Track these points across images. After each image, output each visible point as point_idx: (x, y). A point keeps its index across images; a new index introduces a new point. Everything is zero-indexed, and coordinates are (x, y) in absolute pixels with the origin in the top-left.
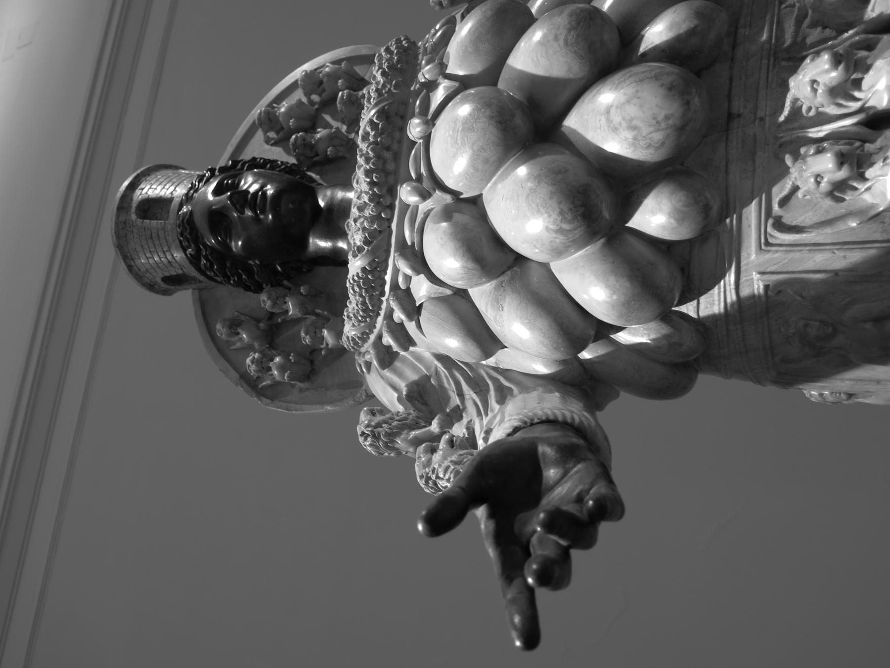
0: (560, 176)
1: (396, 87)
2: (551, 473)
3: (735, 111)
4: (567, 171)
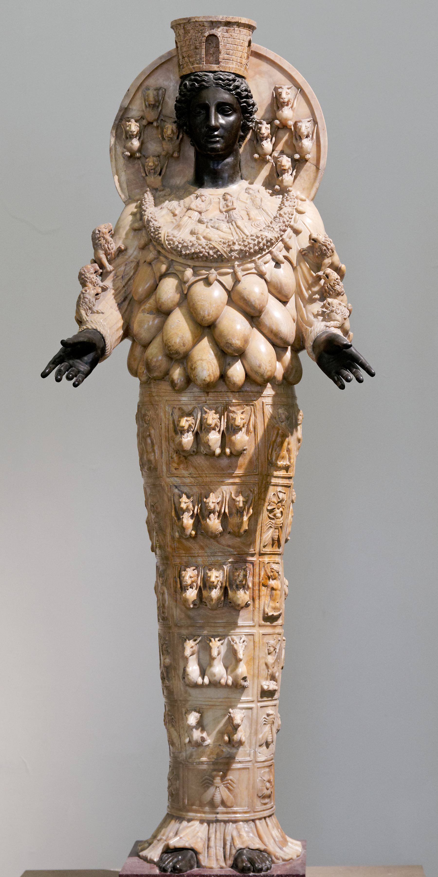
0: (182, 344)
1: (235, 257)
2: (86, 358)
3: (210, 393)
4: (184, 346)
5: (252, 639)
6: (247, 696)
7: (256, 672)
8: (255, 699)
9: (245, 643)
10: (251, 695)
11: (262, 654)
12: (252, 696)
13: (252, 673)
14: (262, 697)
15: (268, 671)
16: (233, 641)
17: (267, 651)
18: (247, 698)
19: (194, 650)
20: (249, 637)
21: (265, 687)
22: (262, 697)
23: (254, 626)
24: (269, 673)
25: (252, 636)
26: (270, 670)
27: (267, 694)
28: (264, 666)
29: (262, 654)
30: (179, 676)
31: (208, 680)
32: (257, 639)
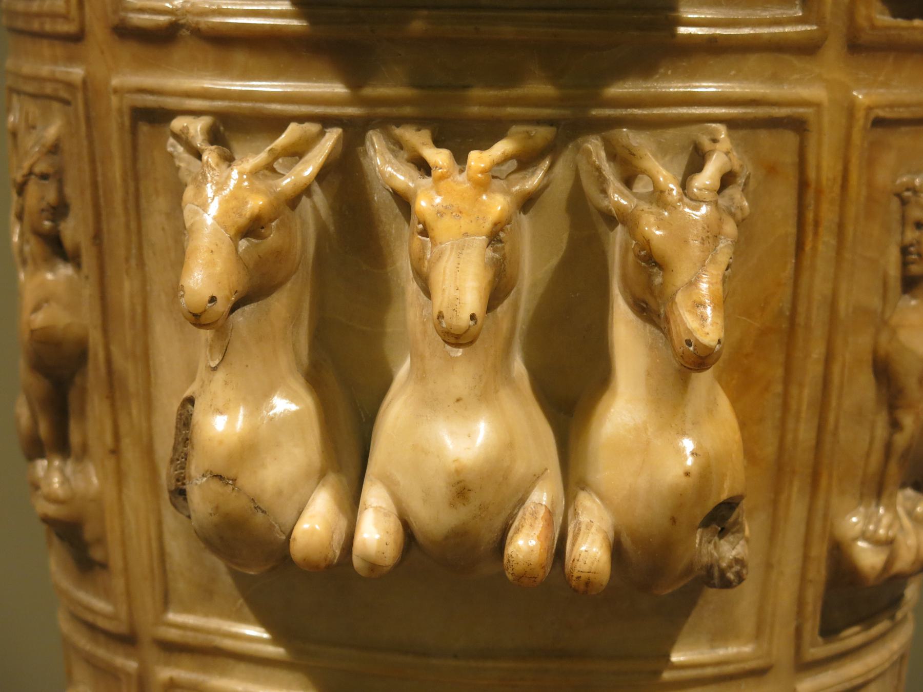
5: (789, 158)
6: (719, 636)
7: (805, 433)
8: (780, 648)
9: (735, 192)
10: (748, 624)
11: (859, 292)
12: (758, 634)
13: (769, 450)
14: (829, 631)
15: (895, 425)
16: (628, 181)
17: (894, 272)
18: (722, 652)
19: (278, 255)
20: (764, 136)
21: (868, 557)
22: (829, 631)
23: (807, 49)
24: (901, 440)
25: (790, 139)
26: (908, 421)
27: (852, 599)
28: (862, 389)
29: (859, 292)
30: (149, 452)
31: (392, 524)
32: (825, 163)
